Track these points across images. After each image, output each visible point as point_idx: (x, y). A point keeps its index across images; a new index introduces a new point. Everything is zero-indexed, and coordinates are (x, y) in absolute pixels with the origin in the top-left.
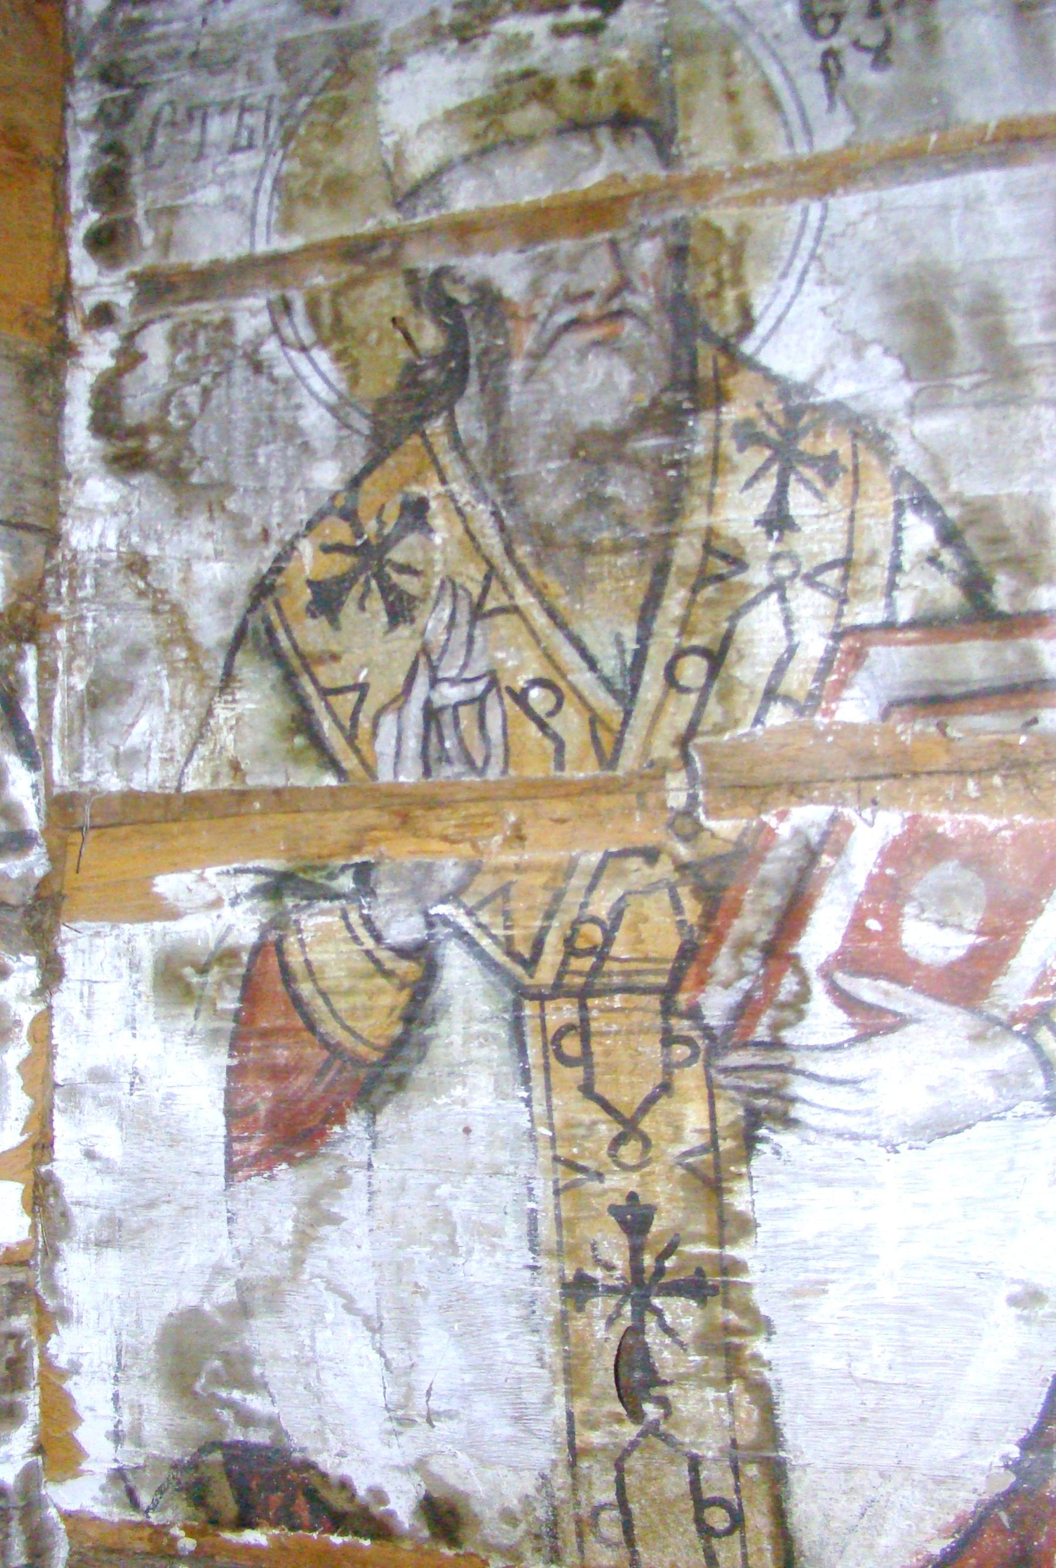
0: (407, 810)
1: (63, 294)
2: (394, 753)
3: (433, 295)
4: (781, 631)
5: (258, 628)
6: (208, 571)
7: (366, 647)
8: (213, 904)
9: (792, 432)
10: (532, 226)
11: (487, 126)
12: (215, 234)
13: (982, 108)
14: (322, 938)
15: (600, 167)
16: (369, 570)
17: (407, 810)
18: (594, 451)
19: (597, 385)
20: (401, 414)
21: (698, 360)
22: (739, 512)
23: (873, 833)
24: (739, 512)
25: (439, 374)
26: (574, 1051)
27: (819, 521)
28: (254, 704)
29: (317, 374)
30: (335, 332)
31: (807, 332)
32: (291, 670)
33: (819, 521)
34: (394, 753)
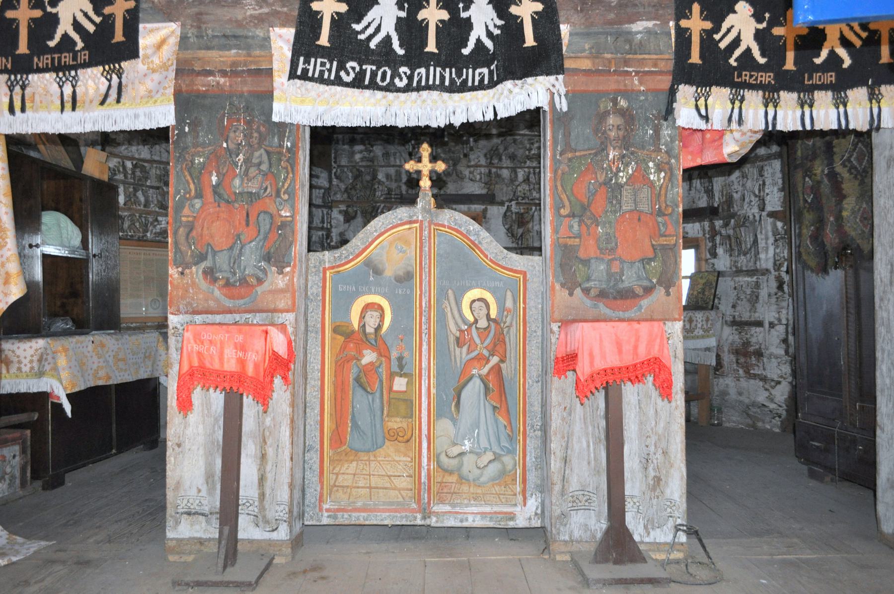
0: (356, 202)
1: (331, 165)
2: (355, 199)
3: (358, 170)
4: (378, 194)
5: (346, 190)
6: (343, 186)
7: (353, 192)
8: (343, 207)
9: (380, 182)
10: (364, 166)
11: (362, 159)
12: (343, 163)
13: (392, 163)
14: (350, 210)
15: (369, 163)
16: (354, 187)
17: (356, 202)
18: (368, 182)
19: (368, 178)
20: (356, 178)
21: (374, 177)
22: (376, 186)
23: (382, 205)
24: (376, 186)
25: (358, 176)
26: (365, 217)
27: (381, 188)
28: (345, 195)
29: (350, 174)
30: (351, 172)
31: (381, 176)
32: (348, 193)
33: (381, 188)
34: (355, 199)
